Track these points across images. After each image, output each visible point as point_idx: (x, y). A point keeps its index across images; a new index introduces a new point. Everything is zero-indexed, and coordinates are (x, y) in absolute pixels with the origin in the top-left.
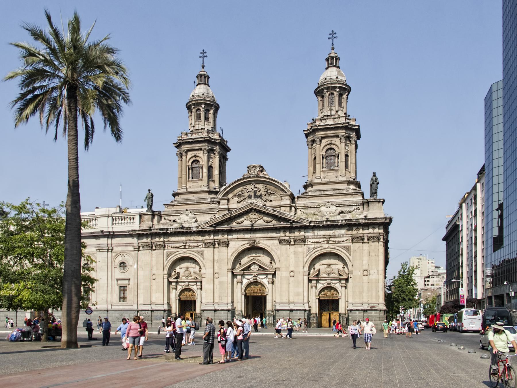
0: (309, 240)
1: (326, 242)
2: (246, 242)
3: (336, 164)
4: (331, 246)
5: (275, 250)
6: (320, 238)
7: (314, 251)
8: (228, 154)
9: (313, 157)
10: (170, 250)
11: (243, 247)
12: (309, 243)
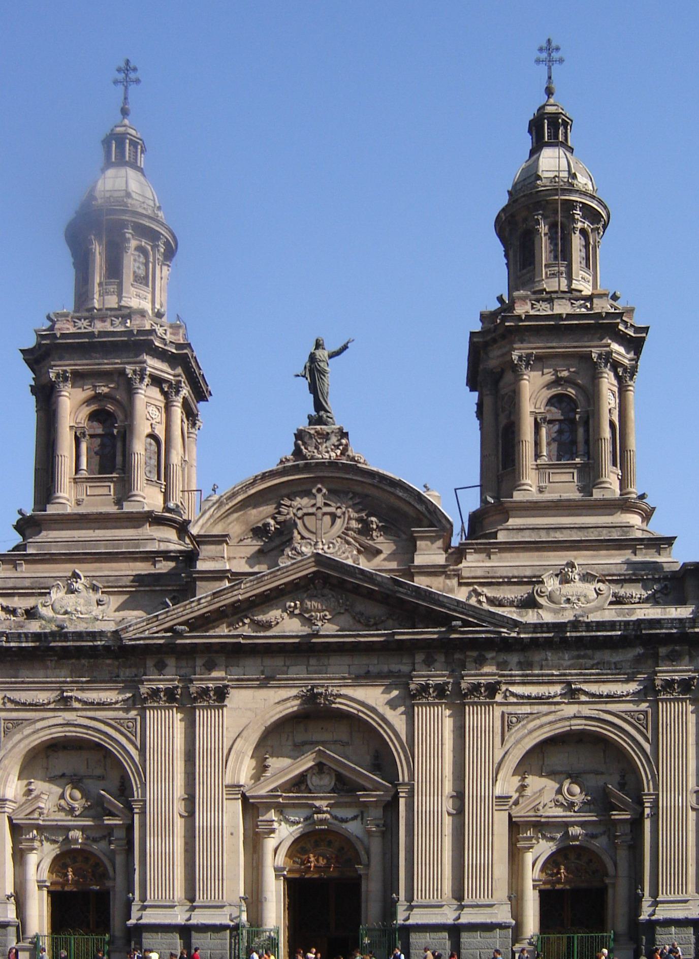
0: (514, 689)
2: (294, 692)
3: (581, 447)
4: (586, 710)
8: (201, 405)
9: (503, 421)
10: (14, 715)
11: (280, 708)
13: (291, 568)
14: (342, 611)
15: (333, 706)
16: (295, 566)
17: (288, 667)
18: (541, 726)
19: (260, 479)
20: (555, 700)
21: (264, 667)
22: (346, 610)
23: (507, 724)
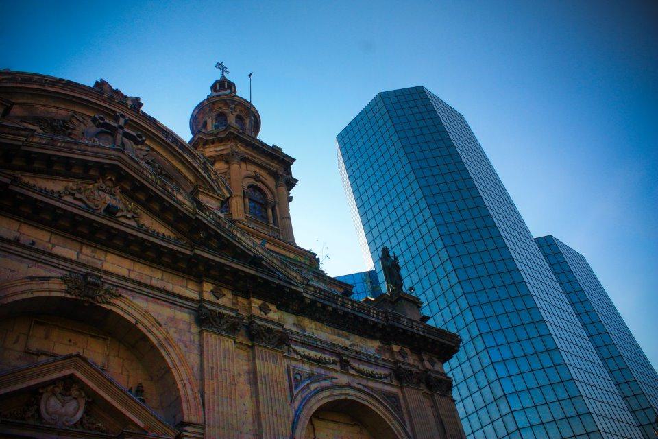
1: (338, 367)
2: (56, 273)
3: (271, 220)
5: (181, 345)
6: (322, 350)
7: (313, 387)
11: (34, 286)
12: (296, 357)
13: (90, 149)
14: (129, 216)
15: (105, 306)
16: (95, 150)
17: (54, 245)
18: (324, 389)
19: (63, 84)
20: (331, 366)
21: (21, 234)
22: (133, 217)
23: (295, 381)
